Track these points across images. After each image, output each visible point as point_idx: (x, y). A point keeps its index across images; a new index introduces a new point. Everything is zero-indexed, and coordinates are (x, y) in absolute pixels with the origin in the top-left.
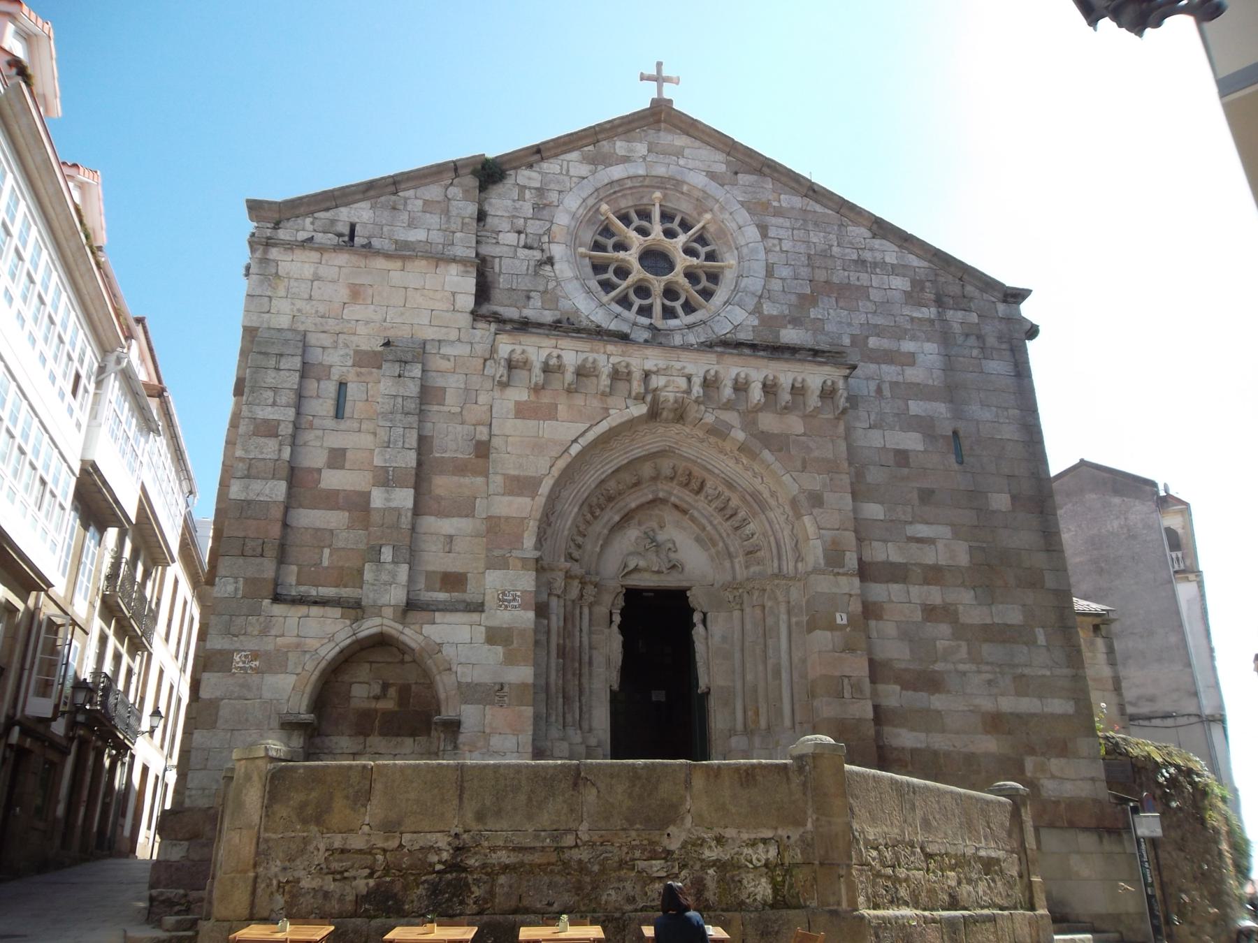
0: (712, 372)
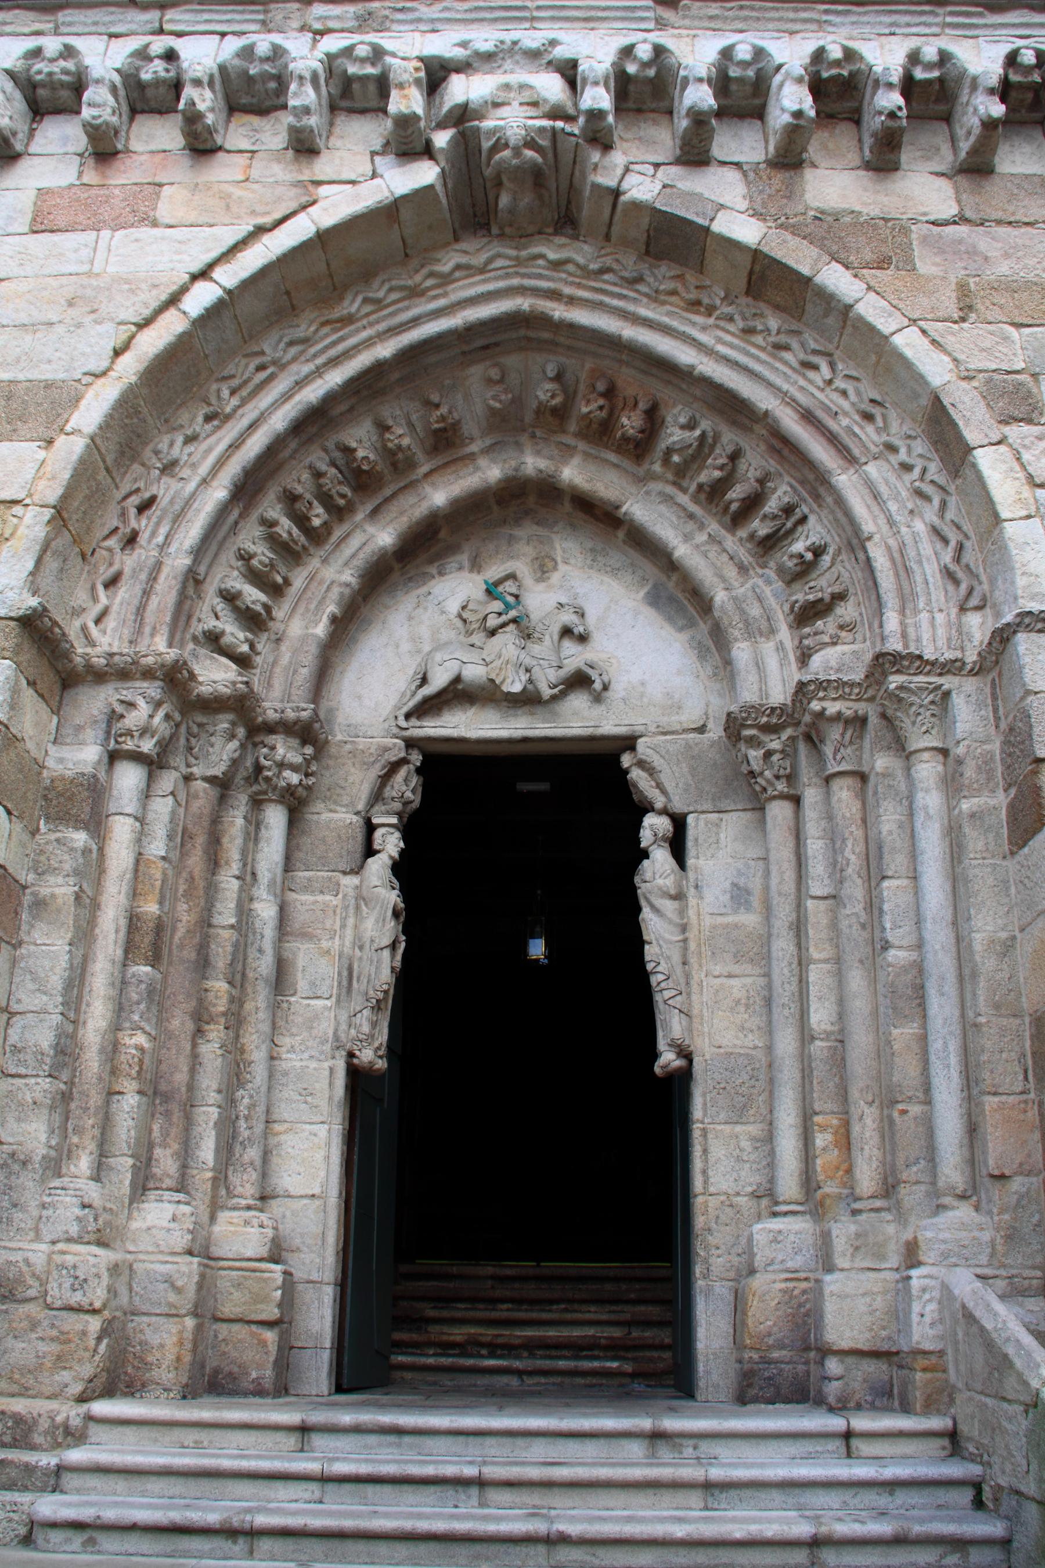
0: (644, 52)
